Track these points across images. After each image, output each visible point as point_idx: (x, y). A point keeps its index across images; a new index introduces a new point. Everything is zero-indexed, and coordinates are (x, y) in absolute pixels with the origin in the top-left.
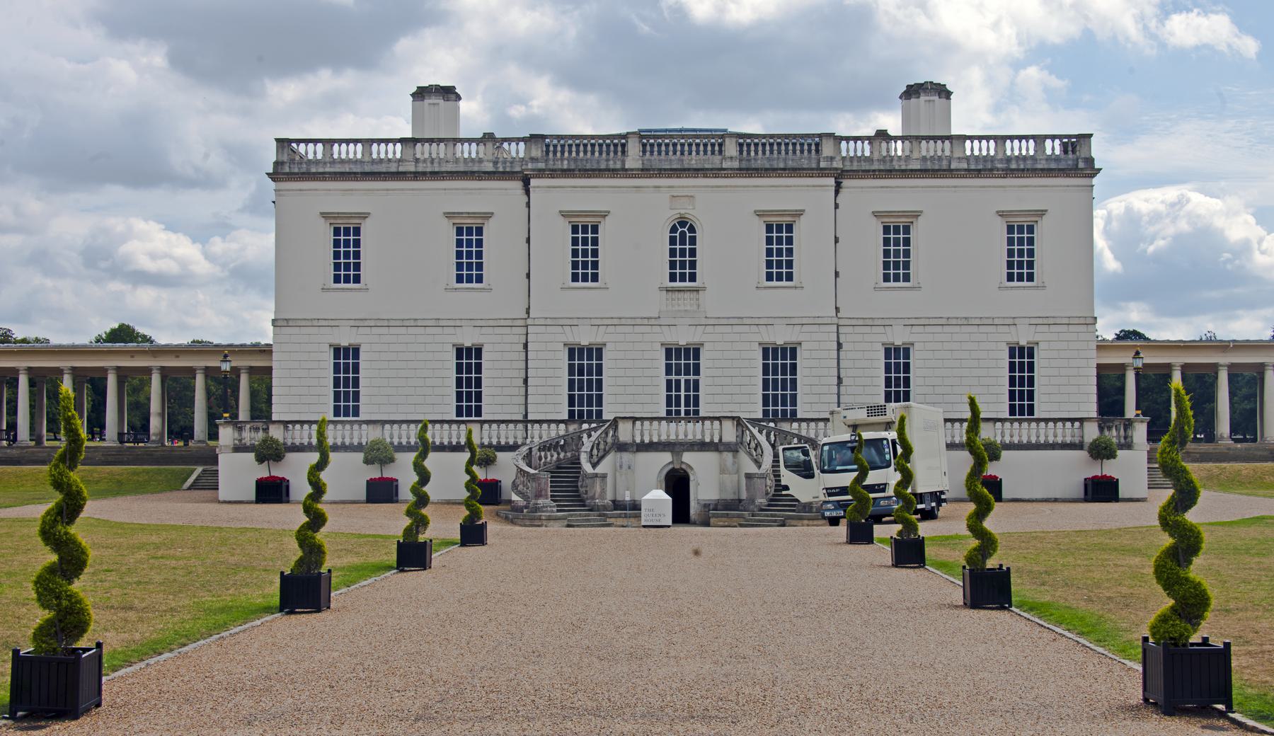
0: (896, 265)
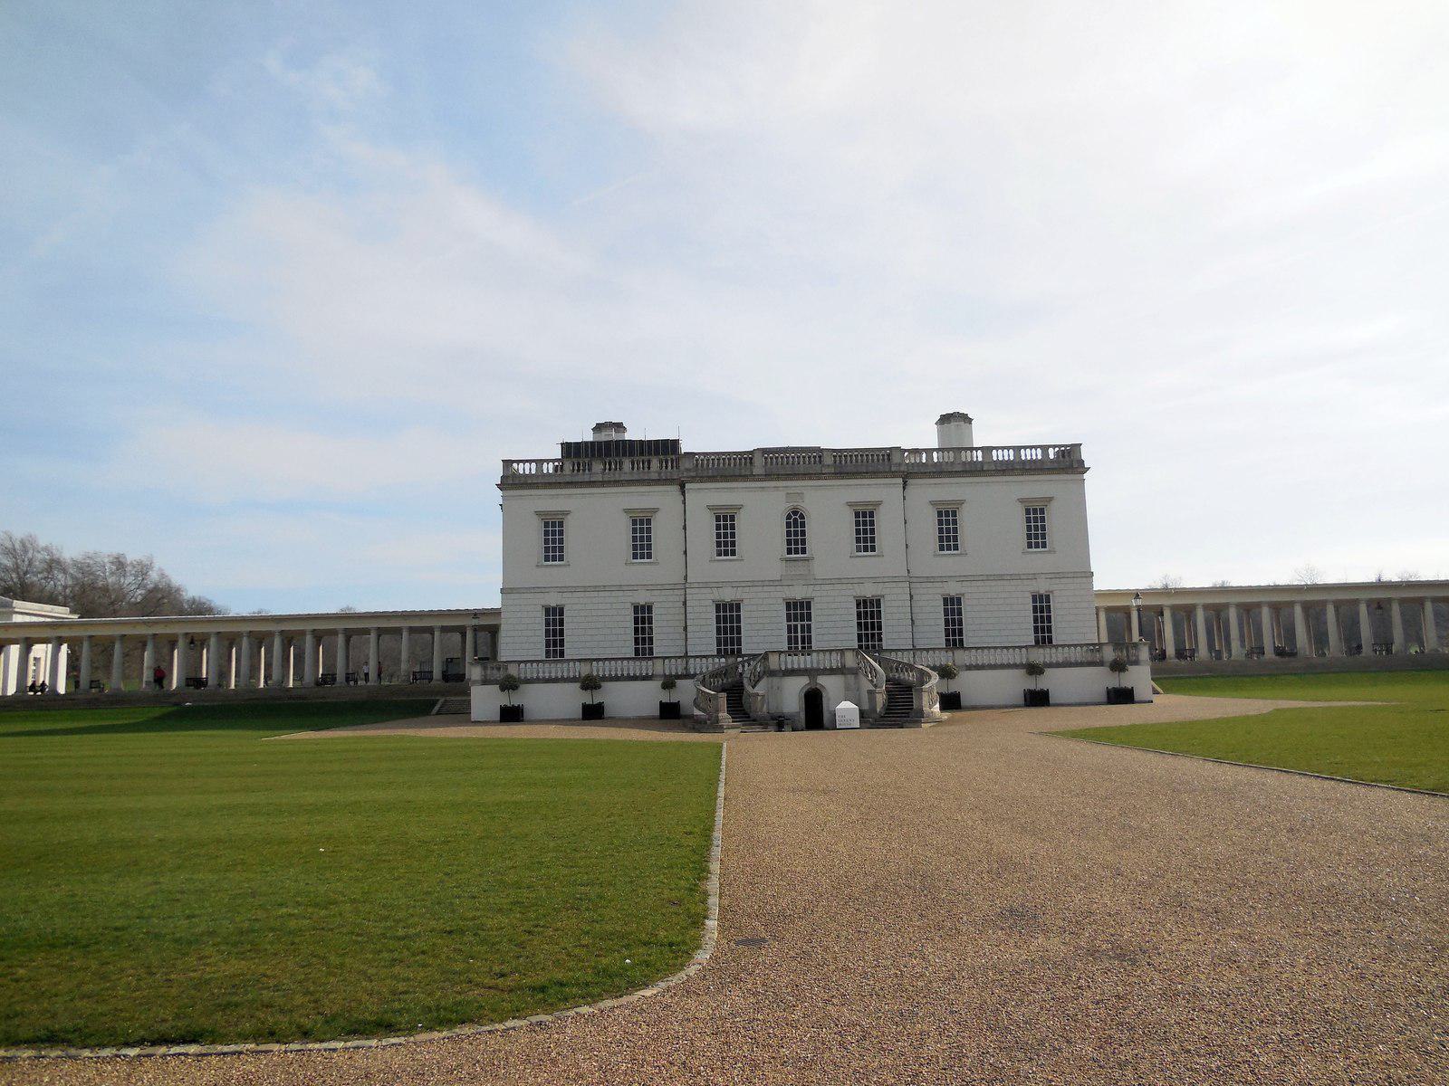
0: (948, 537)
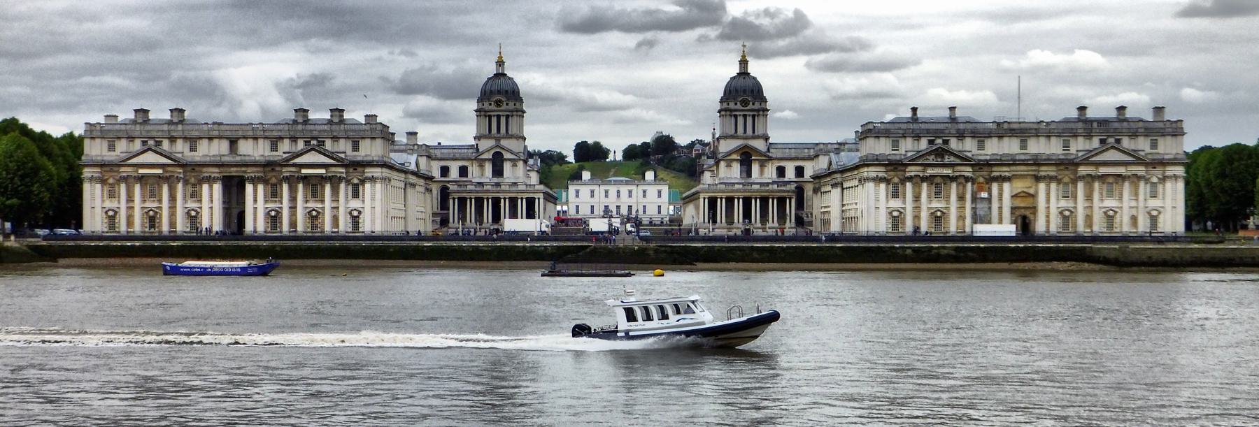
0: (644, 196)
